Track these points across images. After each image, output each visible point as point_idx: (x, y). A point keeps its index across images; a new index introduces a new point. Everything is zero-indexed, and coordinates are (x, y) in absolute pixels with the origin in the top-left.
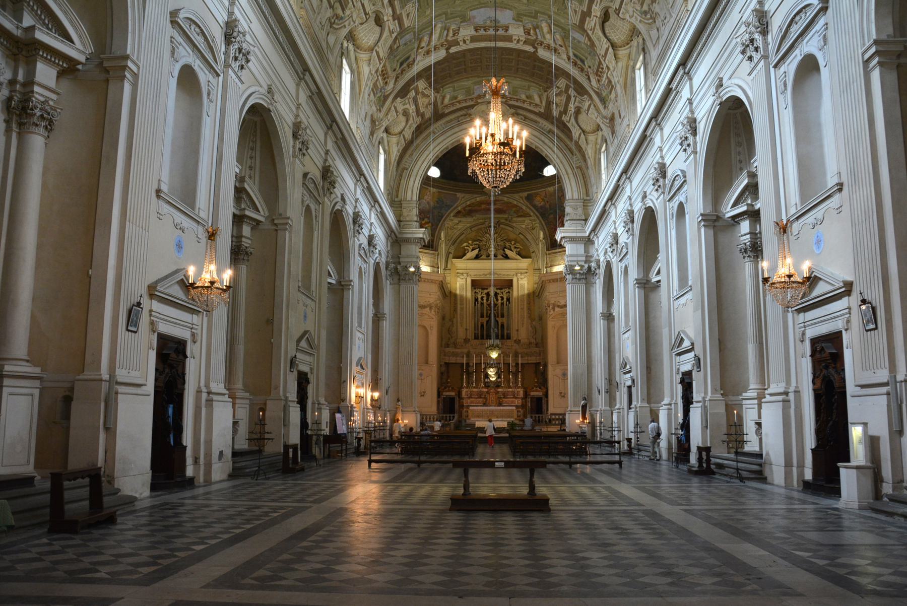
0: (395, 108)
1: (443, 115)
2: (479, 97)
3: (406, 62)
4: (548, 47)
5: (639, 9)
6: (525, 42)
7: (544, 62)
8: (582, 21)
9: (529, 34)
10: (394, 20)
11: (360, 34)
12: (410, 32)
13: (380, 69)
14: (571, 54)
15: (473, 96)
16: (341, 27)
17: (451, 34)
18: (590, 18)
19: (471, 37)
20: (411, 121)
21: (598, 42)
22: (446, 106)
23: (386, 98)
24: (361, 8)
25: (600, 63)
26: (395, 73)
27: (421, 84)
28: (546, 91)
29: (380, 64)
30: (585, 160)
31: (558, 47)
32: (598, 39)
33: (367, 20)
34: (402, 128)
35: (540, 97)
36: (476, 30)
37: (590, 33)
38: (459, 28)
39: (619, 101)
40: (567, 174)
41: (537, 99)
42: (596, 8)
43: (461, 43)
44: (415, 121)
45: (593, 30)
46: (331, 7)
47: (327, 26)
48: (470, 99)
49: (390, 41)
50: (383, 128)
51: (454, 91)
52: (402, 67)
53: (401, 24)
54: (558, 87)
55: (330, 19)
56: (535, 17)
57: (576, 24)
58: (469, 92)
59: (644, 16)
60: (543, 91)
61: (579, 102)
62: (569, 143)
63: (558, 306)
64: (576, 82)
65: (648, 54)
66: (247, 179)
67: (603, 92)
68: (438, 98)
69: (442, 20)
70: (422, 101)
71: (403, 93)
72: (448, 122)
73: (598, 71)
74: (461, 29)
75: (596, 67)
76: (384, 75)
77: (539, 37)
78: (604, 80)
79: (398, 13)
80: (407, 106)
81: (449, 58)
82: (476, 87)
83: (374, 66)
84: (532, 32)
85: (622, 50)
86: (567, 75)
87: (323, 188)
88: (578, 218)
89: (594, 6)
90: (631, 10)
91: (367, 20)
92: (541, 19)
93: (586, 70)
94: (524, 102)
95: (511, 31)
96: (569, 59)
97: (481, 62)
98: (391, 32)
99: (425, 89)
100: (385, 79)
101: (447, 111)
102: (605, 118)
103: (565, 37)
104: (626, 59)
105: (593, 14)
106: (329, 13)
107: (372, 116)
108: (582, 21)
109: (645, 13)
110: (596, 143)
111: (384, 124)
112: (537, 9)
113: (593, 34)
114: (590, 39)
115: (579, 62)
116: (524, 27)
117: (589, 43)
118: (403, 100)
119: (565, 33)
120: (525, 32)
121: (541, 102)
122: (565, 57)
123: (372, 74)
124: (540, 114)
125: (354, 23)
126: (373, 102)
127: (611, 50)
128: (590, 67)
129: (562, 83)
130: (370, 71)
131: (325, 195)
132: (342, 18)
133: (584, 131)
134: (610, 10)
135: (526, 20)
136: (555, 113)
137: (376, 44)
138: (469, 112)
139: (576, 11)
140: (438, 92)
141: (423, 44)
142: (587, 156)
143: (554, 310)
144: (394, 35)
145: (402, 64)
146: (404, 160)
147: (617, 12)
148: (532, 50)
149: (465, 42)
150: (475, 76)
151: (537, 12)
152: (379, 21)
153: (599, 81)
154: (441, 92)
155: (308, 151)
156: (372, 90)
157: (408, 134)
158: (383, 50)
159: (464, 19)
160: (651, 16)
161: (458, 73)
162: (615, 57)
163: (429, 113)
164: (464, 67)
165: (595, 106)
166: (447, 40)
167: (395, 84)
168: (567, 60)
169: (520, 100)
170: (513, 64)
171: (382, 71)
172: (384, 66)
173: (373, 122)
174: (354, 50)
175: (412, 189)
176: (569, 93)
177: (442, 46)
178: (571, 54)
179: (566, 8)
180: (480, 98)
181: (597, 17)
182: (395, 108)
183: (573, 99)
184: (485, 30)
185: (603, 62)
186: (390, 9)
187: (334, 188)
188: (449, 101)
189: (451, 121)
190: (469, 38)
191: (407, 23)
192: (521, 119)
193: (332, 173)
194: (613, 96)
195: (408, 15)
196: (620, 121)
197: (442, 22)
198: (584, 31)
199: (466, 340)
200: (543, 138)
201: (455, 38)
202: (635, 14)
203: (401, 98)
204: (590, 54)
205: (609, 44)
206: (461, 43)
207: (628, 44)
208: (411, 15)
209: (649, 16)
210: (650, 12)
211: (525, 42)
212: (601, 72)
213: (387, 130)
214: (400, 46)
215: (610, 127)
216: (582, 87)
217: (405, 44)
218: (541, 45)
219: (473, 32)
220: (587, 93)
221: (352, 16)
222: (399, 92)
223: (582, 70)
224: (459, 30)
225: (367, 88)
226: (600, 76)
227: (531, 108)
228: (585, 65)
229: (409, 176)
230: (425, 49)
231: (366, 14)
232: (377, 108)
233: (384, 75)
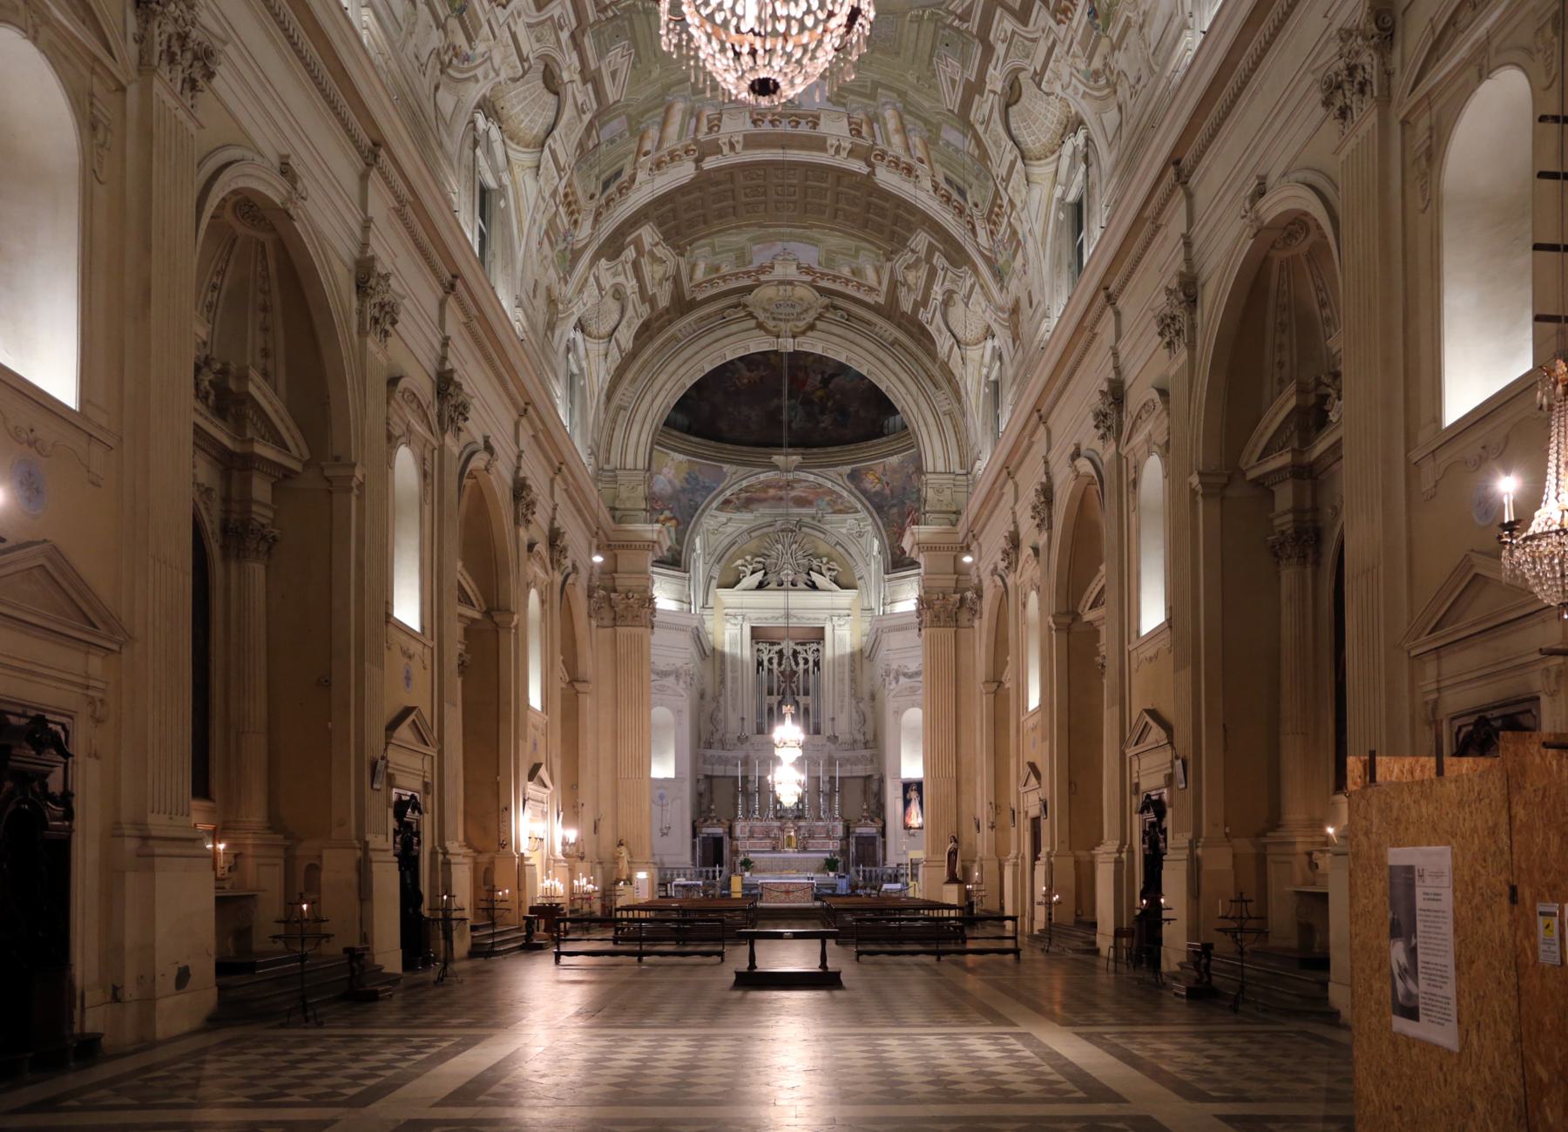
0: (597, 280)
1: (693, 305)
2: (762, 270)
3: (614, 183)
4: (896, 163)
5: (1083, 67)
6: (851, 153)
7: (886, 195)
8: (966, 104)
9: (859, 133)
10: (585, 82)
11: (513, 106)
12: (620, 115)
13: (561, 191)
14: (940, 179)
15: (750, 268)
16: (468, 79)
17: (704, 128)
18: (982, 96)
19: (745, 136)
20: (630, 312)
21: (994, 148)
22: (698, 285)
23: (576, 255)
24: (510, 41)
25: (997, 191)
27: (648, 234)
28: (889, 260)
29: (561, 179)
30: (959, 400)
32: (995, 143)
33: (525, 73)
34: (613, 324)
35: (877, 271)
36: (754, 122)
37: (980, 129)
38: (721, 114)
39: (1030, 273)
40: (926, 425)
42: (996, 73)
43: (726, 149)
44: (638, 313)
45: (986, 122)
46: (441, 26)
47: (434, 68)
48: (744, 273)
51: (715, 253)
52: (609, 191)
53: (599, 92)
54: (913, 251)
55: (438, 54)
56: (873, 96)
57: (952, 111)
58: (742, 257)
59: (1092, 83)
60: (882, 259)
61: (953, 281)
62: (929, 365)
63: (905, 675)
65: (1094, 166)
66: (254, 374)
67: (999, 256)
68: (682, 267)
69: (686, 93)
70: (651, 271)
71: (612, 247)
72: (702, 319)
73: (991, 212)
74: (724, 117)
75: (988, 204)
76: (569, 204)
77: (879, 141)
78: (1002, 232)
79: (593, 67)
80: (621, 279)
81: (703, 180)
82: (755, 248)
83: (547, 181)
84: (865, 129)
85: (1040, 166)
87: (440, 416)
88: (944, 508)
89: (991, 69)
90: (1065, 71)
91: (525, 73)
92: (884, 100)
93: (968, 211)
94: (847, 282)
95: (825, 127)
96: (936, 188)
97: (765, 194)
98: (581, 111)
99: (657, 244)
100: (572, 213)
101: (700, 297)
102: (1002, 310)
104: (1047, 184)
105: (988, 87)
106: (436, 39)
107: (549, 290)
108: (966, 104)
109: (1096, 75)
110: (981, 364)
111: (577, 311)
112: (877, 77)
113: (985, 132)
114: (979, 143)
115: (955, 196)
116: (849, 117)
117: (976, 153)
118: (613, 263)
119: (930, 131)
120: (851, 130)
121: (880, 283)
122: (928, 184)
123: (543, 198)
125: (498, 75)
126: (549, 259)
127: (1019, 164)
128: (976, 205)
129: (921, 240)
130: (540, 191)
131: (443, 431)
132: (467, 59)
134: (1022, 76)
136: (906, 306)
137: (549, 133)
138: (743, 300)
139: (953, 82)
140: (682, 255)
141: (648, 145)
142: (963, 392)
143: (897, 682)
144: (587, 118)
145: (606, 185)
147: (1037, 79)
148: (865, 170)
149: (732, 146)
150: (754, 225)
151: (876, 85)
152: (551, 81)
153: (992, 233)
154: (687, 254)
155: (397, 326)
156: (546, 233)
157: (626, 336)
158: (563, 145)
160: (1108, 80)
161: (721, 215)
162: (1027, 179)
163: (664, 301)
164: (731, 202)
165: (982, 287)
167: (593, 228)
168: (932, 192)
169: (840, 278)
170: (827, 202)
171: (566, 195)
172: (569, 185)
173: (552, 302)
174: (503, 141)
176: (934, 261)
177: (687, 152)
178: (940, 179)
179: (934, 76)
180: (763, 273)
181: (995, 93)
182: (597, 280)
183: (941, 273)
184: (772, 122)
185: (1002, 192)
186: (575, 57)
187: (466, 419)
188: (705, 273)
189: (709, 316)
190: (741, 139)
191: (612, 93)
192: (842, 317)
193: (459, 386)
194: (1019, 260)
195: (614, 74)
196: (1031, 312)
197: (685, 98)
200: (882, 354)
201: (713, 136)
202: (1074, 80)
203: (610, 259)
204: (977, 177)
205: (1016, 152)
206: (726, 149)
207: (1053, 152)
208: (621, 77)
209: (1102, 82)
210: (1107, 72)
211: (851, 153)
212: (997, 215)
213: (581, 326)
214: (599, 144)
215: (1008, 328)
216: (960, 249)
217: (612, 141)
218: (883, 159)
219: (749, 127)
220: (968, 260)
221: (490, 58)
222: (601, 247)
223: (961, 212)
224: (720, 120)
225: (535, 229)
226: (995, 223)
227: (860, 295)
228: (966, 200)
231: (522, 59)
232: (558, 274)
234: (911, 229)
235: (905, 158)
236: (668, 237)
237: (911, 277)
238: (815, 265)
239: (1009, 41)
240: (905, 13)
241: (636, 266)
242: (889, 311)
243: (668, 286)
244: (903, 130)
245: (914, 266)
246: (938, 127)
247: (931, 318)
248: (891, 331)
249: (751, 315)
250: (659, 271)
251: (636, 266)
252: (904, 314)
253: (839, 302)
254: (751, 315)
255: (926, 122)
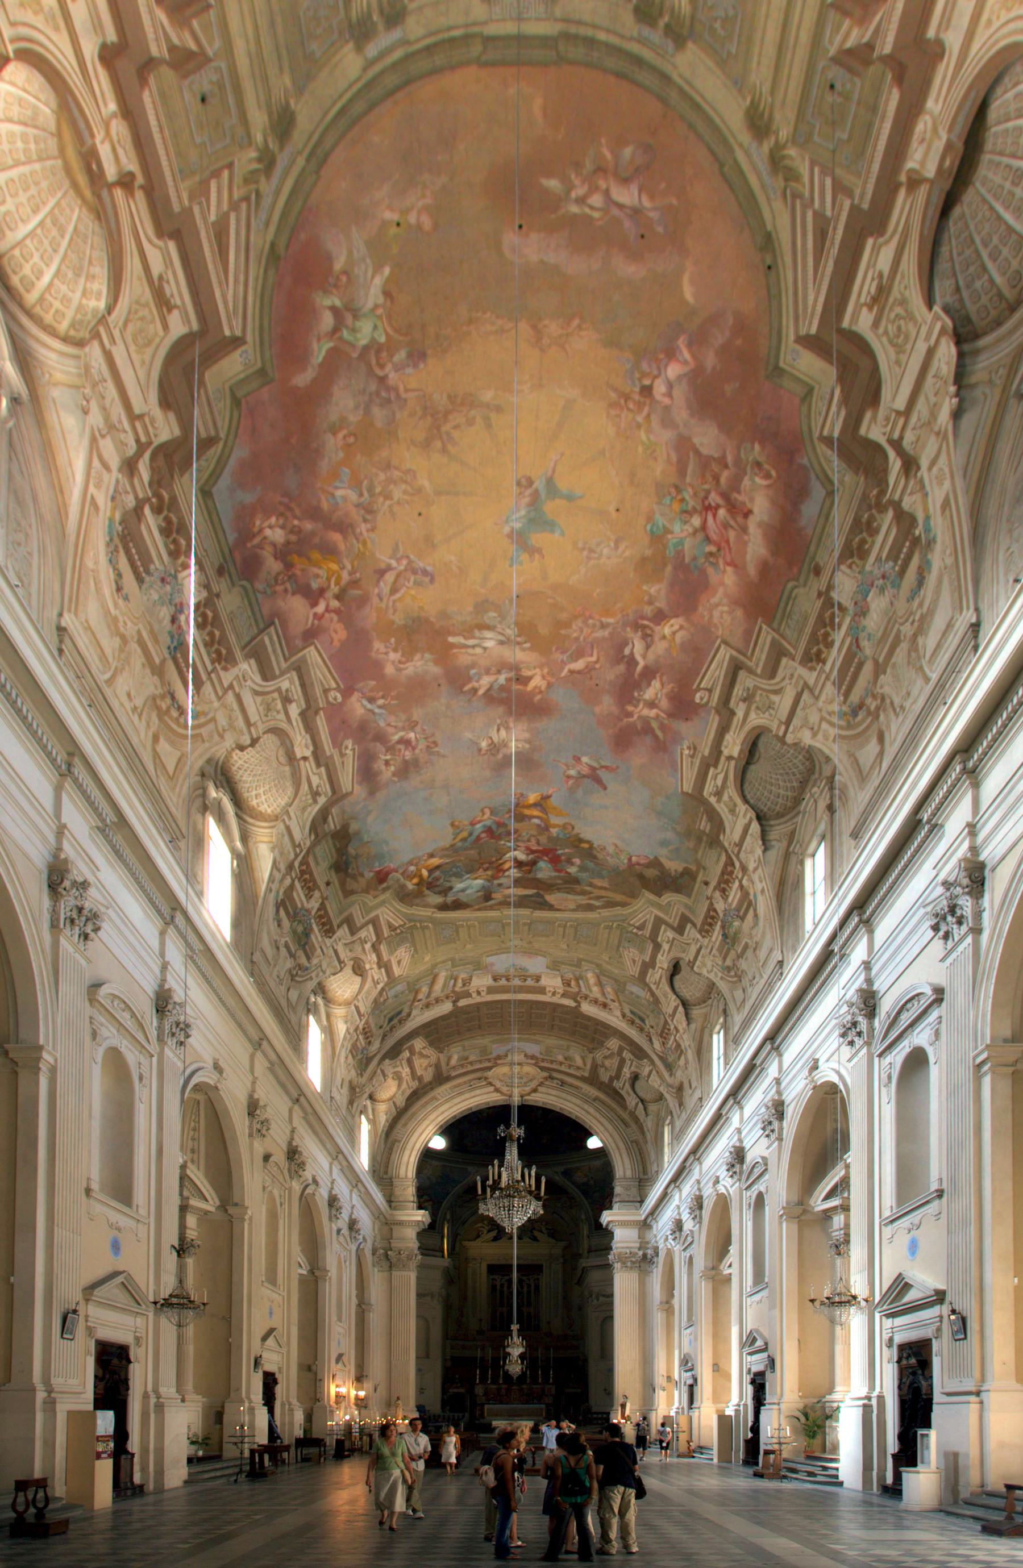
0: (383, 1072)
1: (449, 1079)
3: (397, 1018)
4: (596, 1001)
6: (563, 995)
7: (589, 1018)
9: (569, 985)
17: (460, 983)
20: (404, 1086)
22: (454, 1068)
26: (381, 1031)
27: (419, 1043)
30: (643, 1133)
31: (608, 1001)
35: (583, 1058)
41: (579, 1061)
43: (474, 995)
44: (410, 1085)
49: (375, 993)
50: (366, 1095)
56: (578, 964)
58: (484, 1051)
64: (631, 1042)
70: (419, 1063)
72: (455, 1087)
77: (583, 989)
80: (399, 1069)
84: (573, 983)
86: (623, 1037)
95: (544, 982)
96: (624, 1016)
103: (620, 988)
122: (618, 1013)
124: (583, 1079)
129: (613, 1044)
133: (642, 1101)
135: (565, 969)
136: (605, 1077)
139: (634, 961)
141: (420, 996)
146: (396, 1130)
148: (573, 1004)
151: (580, 960)
157: (401, 1101)
159: (478, 966)
163: (428, 1076)
166: (453, 992)
175: (407, 1165)
177: (447, 997)
183: (628, 1062)
189: (459, 1085)
191: (397, 971)
198: (646, 985)
199: (480, 1332)
208: (404, 963)
211: (563, 995)
227: (572, 1071)
229: (403, 1149)
230: (424, 1001)
233: (367, 1033)
234: (607, 1037)
235: (601, 999)
236: (431, 1044)
237: (607, 1063)
238: (538, 1055)
239: (672, 943)
240: (599, 924)
241: (410, 1062)
242: (593, 1079)
243: (431, 1071)
244: (599, 983)
245: (610, 1056)
246: (625, 984)
247: (622, 1084)
248: (593, 1092)
249: (491, 1084)
250: (425, 1062)
251: (410, 1062)
252: (602, 1083)
253: (555, 1075)
254: (491, 1084)
255: (616, 981)
